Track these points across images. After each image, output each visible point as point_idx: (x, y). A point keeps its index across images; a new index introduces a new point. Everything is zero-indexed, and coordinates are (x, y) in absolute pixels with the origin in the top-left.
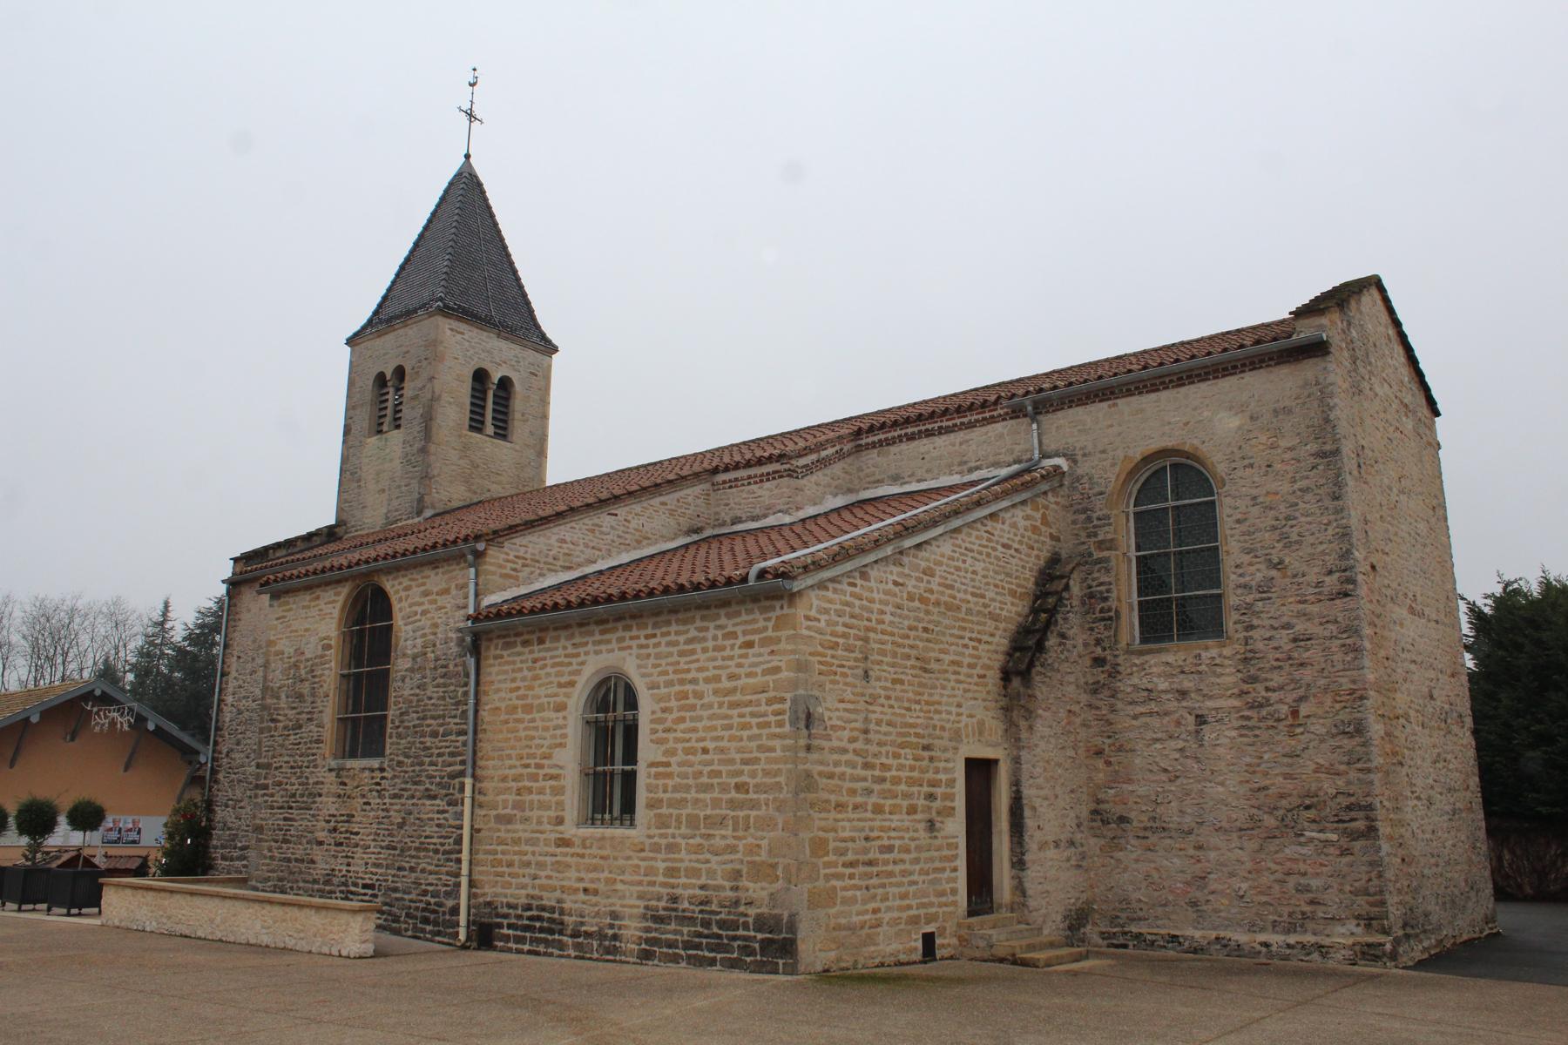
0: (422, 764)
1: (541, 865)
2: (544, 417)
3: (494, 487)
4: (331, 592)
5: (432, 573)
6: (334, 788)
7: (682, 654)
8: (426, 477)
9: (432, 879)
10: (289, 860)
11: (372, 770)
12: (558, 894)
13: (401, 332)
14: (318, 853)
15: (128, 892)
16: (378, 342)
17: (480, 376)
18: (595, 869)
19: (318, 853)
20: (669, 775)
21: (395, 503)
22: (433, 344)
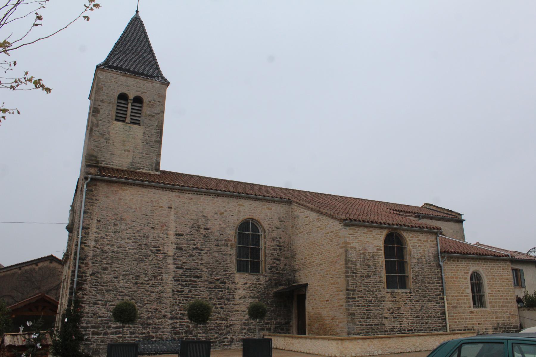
0: (426, 291)
1: (467, 319)
4: (379, 231)
5: (421, 235)
6: (391, 299)
7: (491, 269)
9: (434, 325)
10: (372, 325)
11: (406, 293)
12: (472, 325)
14: (385, 321)
15: (360, 341)
18: (480, 318)
19: (385, 321)
20: (493, 296)
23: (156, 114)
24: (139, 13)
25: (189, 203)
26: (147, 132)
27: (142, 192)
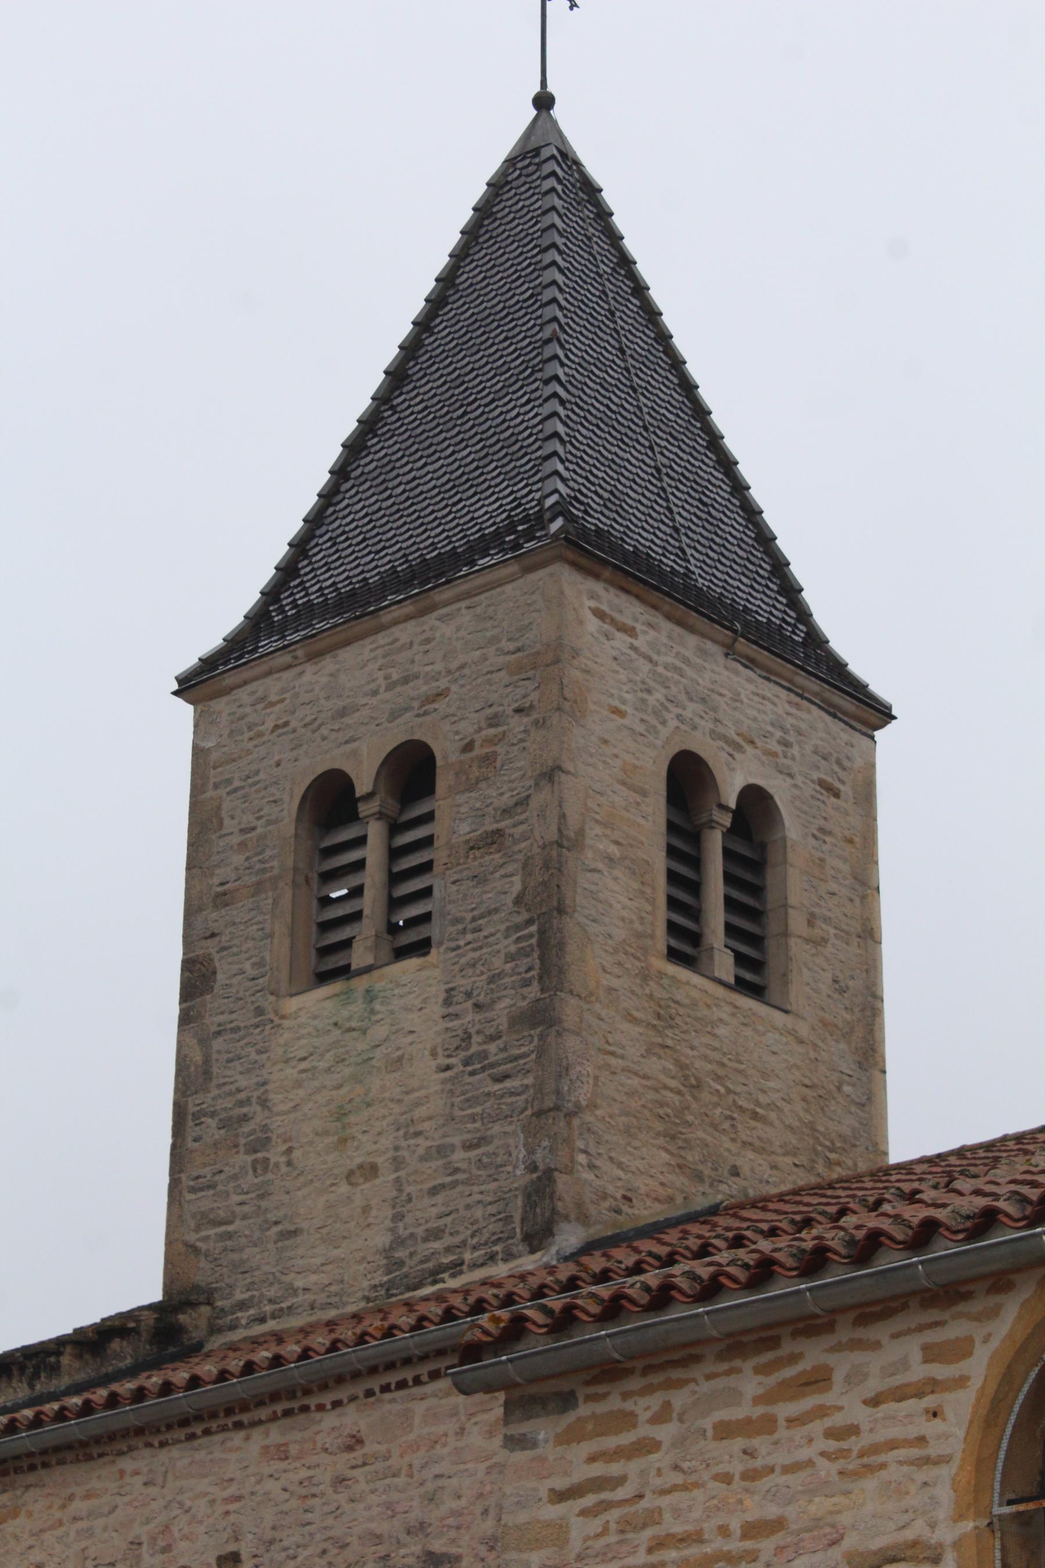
2: (868, 934)
3: (747, 1160)
4: (912, 1348)
8: (550, 1111)
13: (404, 633)
16: (313, 677)
17: (687, 779)
21: (427, 1211)
22: (546, 663)
23: (506, 812)
24: (557, 112)
25: (340, 1481)
26: (463, 983)
27: (88, 1496)
